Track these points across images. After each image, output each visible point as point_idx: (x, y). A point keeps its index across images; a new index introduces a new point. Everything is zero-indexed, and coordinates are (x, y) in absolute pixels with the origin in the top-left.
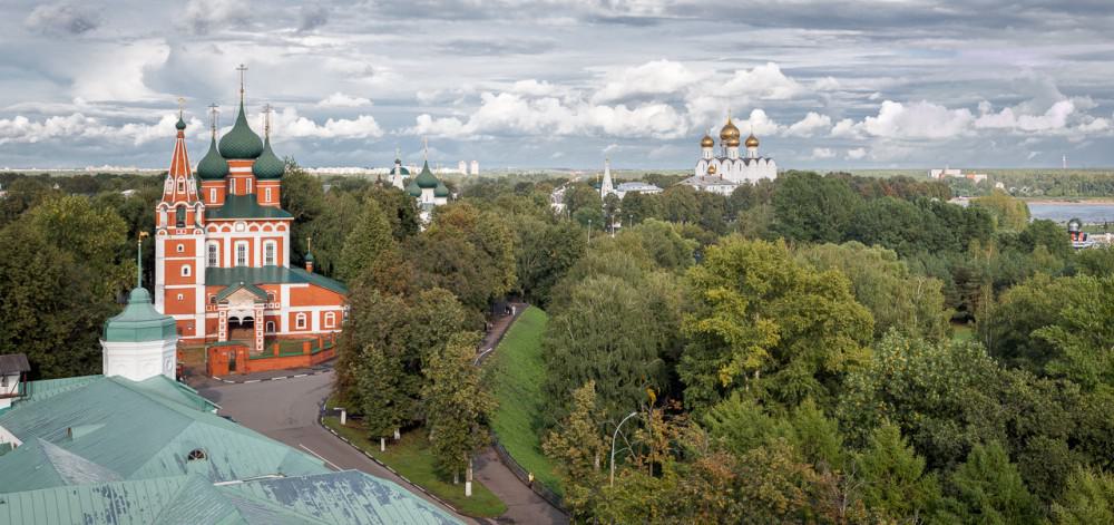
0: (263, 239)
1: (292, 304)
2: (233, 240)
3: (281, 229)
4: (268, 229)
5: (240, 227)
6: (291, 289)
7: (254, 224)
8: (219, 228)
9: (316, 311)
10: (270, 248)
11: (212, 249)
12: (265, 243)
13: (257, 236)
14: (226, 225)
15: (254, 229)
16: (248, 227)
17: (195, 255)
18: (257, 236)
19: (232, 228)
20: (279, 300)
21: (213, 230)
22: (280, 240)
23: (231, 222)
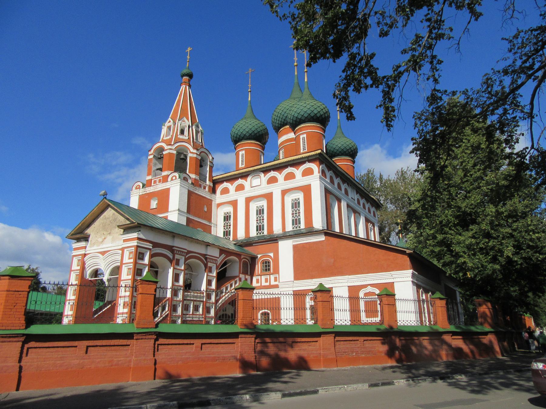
0: (284, 193)
1: (299, 274)
2: (248, 200)
3: (308, 172)
4: (291, 176)
6: (295, 247)
7: (272, 174)
9: (340, 286)
10: (296, 205)
11: (227, 218)
12: (289, 199)
13: (276, 190)
14: (240, 181)
17: (166, 210)
18: (276, 190)
20: (276, 271)
21: (225, 191)
22: (306, 190)
23: (244, 176)
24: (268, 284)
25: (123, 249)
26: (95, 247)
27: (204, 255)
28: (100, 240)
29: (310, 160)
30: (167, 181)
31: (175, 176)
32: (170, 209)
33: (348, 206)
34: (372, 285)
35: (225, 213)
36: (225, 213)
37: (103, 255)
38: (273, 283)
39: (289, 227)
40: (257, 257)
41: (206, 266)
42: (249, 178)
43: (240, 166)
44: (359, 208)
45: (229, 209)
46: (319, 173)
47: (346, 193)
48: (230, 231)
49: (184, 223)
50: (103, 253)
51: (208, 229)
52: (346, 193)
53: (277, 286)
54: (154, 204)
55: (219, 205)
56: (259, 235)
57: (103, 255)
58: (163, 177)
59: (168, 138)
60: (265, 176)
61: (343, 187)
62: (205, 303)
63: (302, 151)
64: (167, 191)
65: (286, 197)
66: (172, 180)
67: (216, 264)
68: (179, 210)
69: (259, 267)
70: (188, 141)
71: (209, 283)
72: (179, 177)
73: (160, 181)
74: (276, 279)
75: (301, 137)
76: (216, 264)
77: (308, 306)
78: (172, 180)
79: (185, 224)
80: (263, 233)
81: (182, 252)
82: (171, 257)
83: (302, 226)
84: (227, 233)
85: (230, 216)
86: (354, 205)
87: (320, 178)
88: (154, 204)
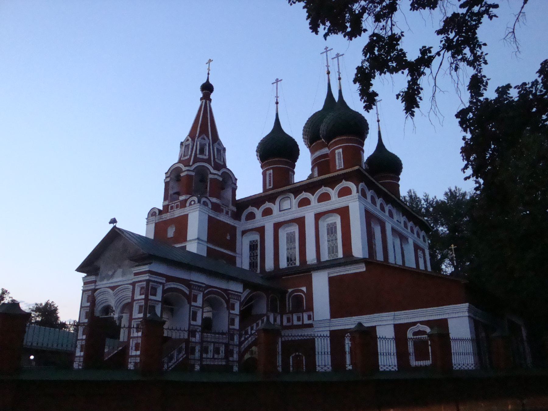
0: (318, 216)
1: (337, 311)
2: (277, 226)
3: (345, 192)
4: (325, 197)
5: (286, 204)
6: (332, 280)
7: (304, 195)
8: (258, 212)
9: (384, 325)
10: (331, 230)
11: (253, 247)
14: (267, 205)
15: (305, 203)
16: (295, 201)
19: (275, 208)
20: (310, 308)
22: (344, 212)
24: (300, 323)
25: (133, 284)
26: (105, 282)
27: (226, 291)
28: (110, 273)
29: (347, 177)
30: (186, 207)
31: (194, 201)
32: (189, 237)
33: (394, 230)
34: (422, 323)
35: (251, 242)
36: (251, 242)
37: (113, 291)
38: (306, 321)
39: (325, 257)
40: (287, 292)
41: (227, 302)
42: (277, 202)
43: (268, 187)
44: (407, 232)
45: (256, 237)
46: (358, 192)
47: (391, 215)
48: (257, 263)
49: (205, 254)
50: (113, 288)
51: (232, 260)
52: (391, 215)
53: (310, 326)
54: (171, 232)
55: (244, 233)
56: (290, 266)
57: (113, 291)
58: (181, 202)
59: (186, 158)
60: (295, 198)
61: (387, 208)
62: (227, 345)
63: (338, 168)
64: (186, 217)
65: (320, 222)
66: (190, 204)
67: (240, 301)
68: (198, 239)
69: (289, 304)
70: (208, 161)
71: (232, 322)
72: (199, 202)
73: (177, 207)
74: (309, 318)
75: (337, 151)
76: (240, 301)
77: (347, 349)
78: (190, 204)
79: (205, 255)
80: (295, 264)
81: (200, 287)
82: (188, 292)
83: (340, 255)
84: (253, 265)
85: (257, 245)
86: (400, 228)
87: (359, 198)
88: (171, 232)
